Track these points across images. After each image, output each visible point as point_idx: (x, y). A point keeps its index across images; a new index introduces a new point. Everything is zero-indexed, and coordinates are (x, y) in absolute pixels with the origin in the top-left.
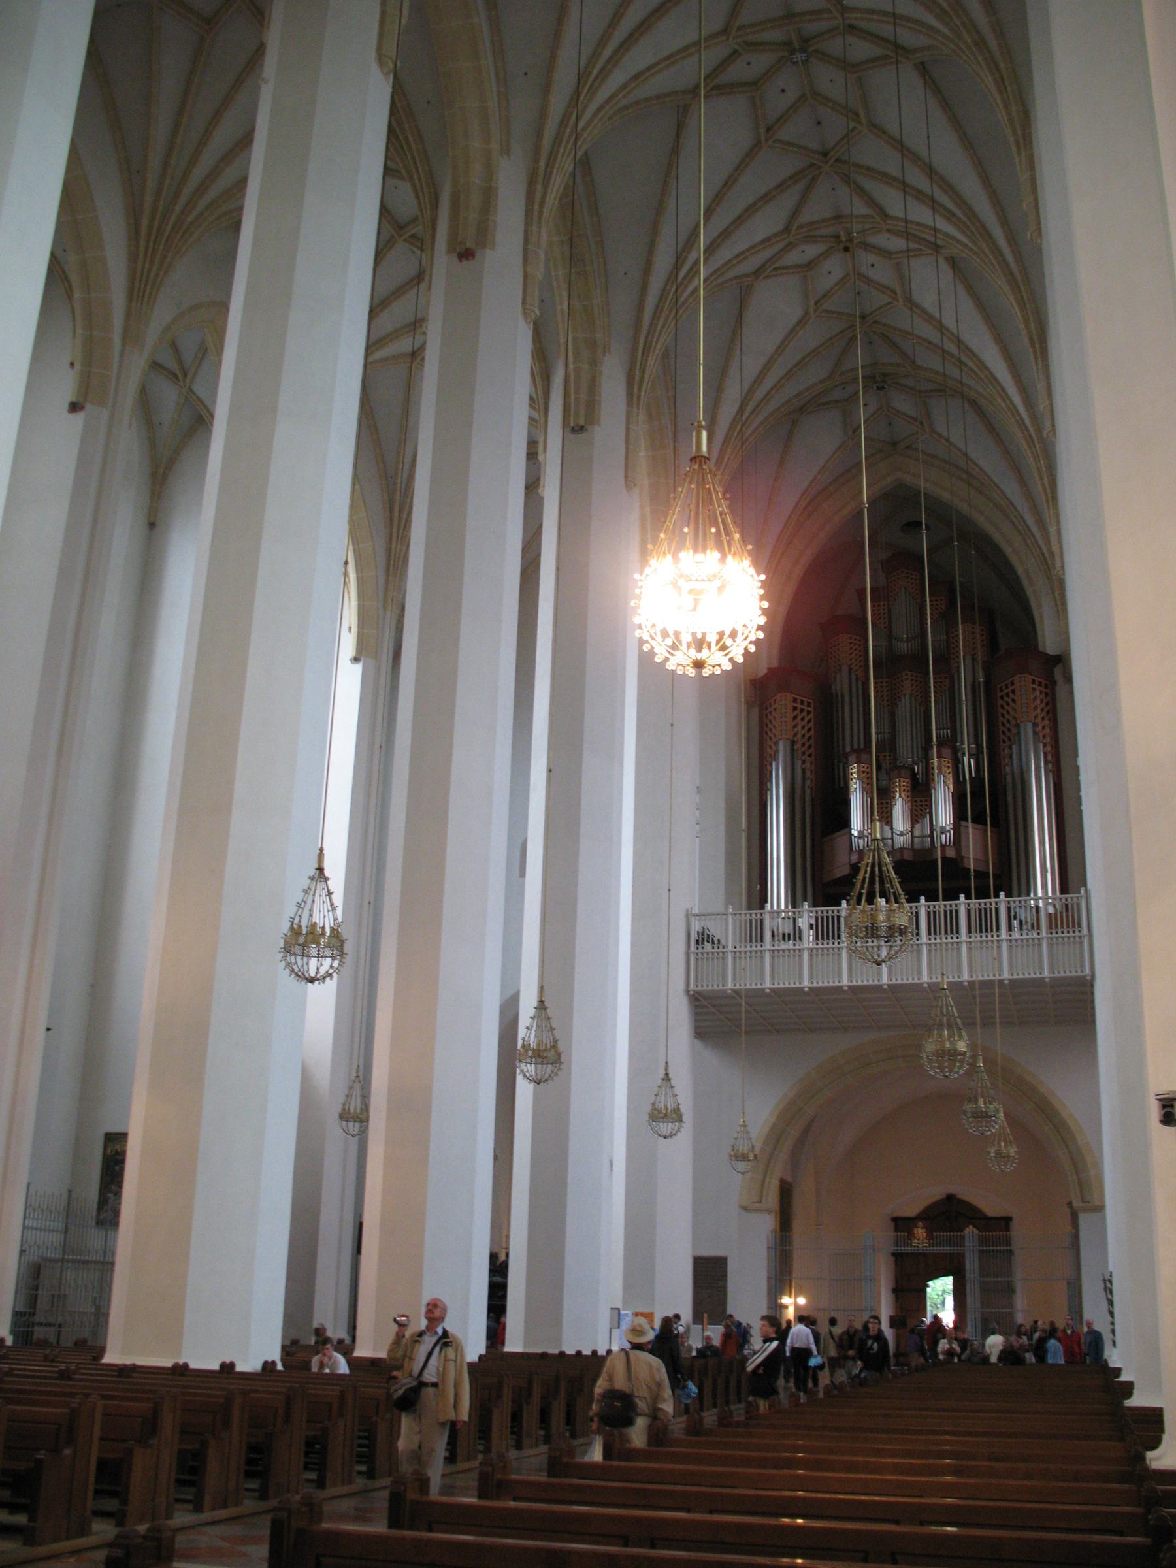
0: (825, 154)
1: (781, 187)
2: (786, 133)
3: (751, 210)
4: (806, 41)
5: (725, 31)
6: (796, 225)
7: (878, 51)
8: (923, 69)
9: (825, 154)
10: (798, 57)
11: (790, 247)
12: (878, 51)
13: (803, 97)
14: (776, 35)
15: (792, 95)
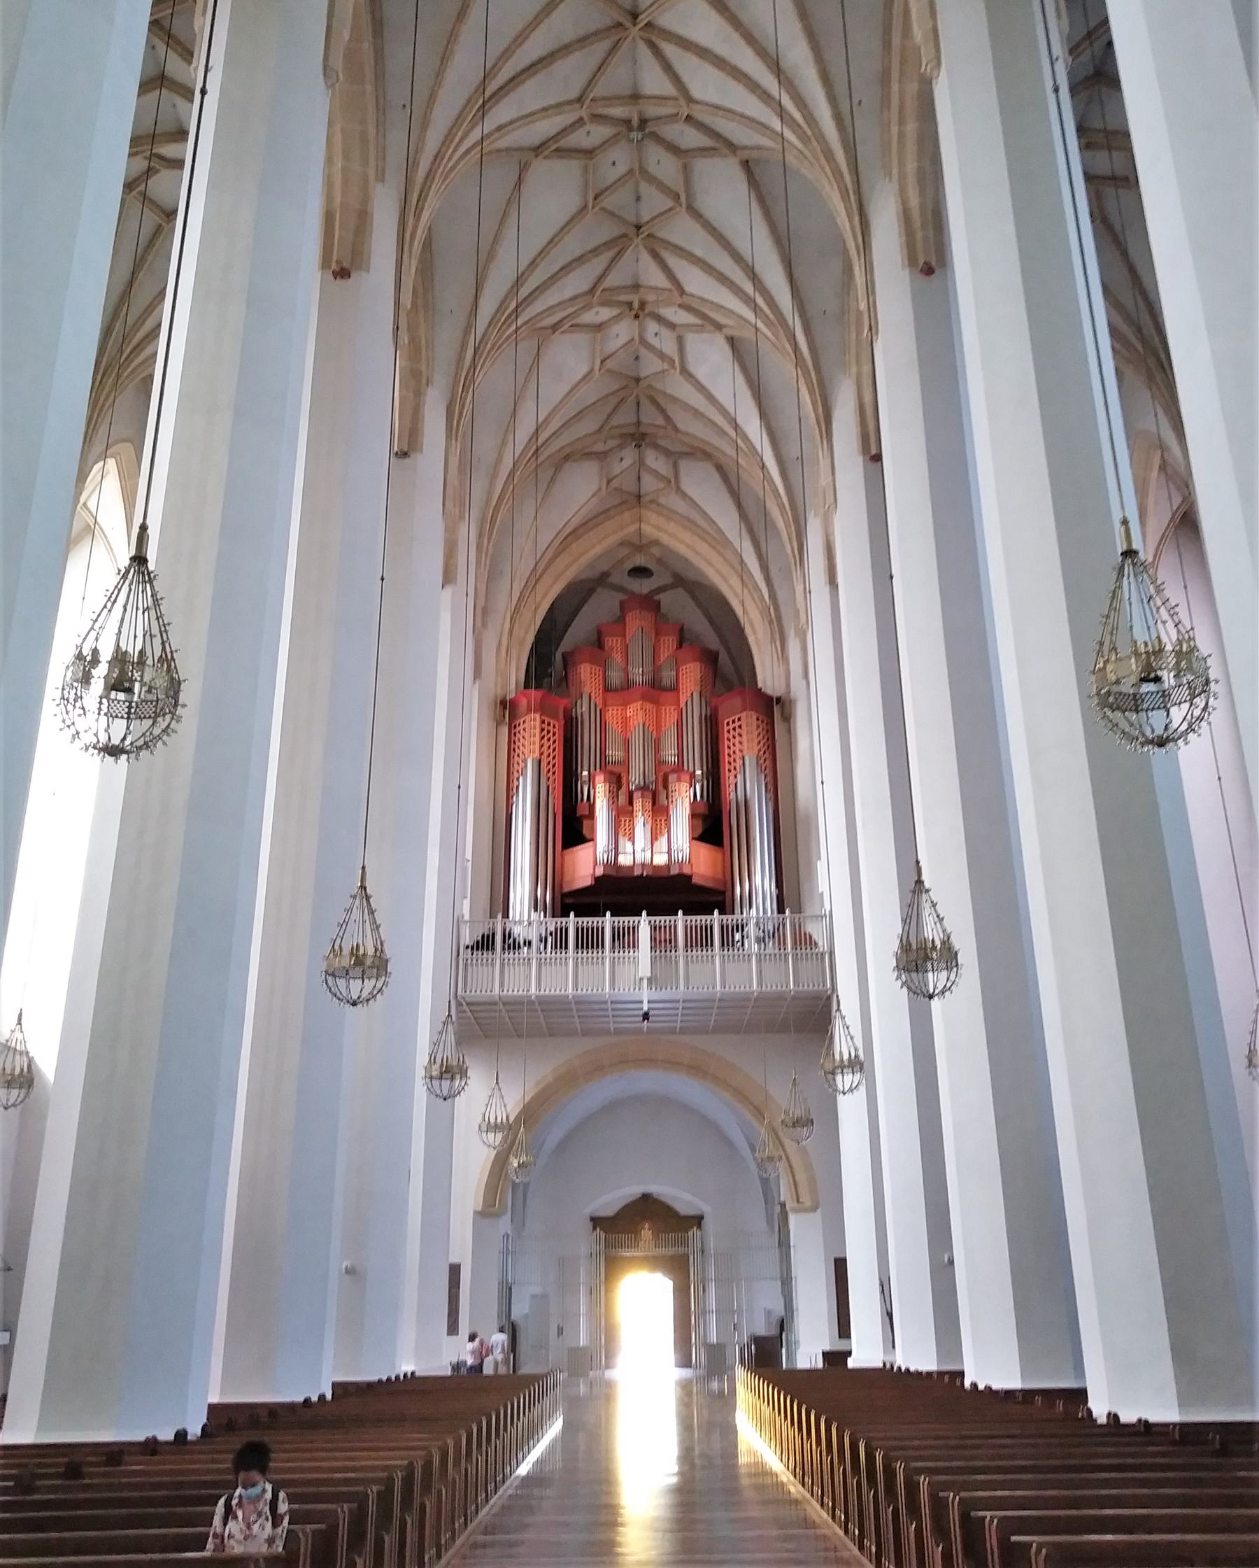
0: (638, 227)
1: (595, 251)
2: (608, 202)
3: (566, 269)
4: (643, 122)
5: (580, 100)
6: (601, 288)
7: (705, 141)
8: (746, 165)
9: (638, 227)
10: (635, 135)
11: (587, 307)
12: (705, 141)
13: (631, 171)
14: (618, 111)
15: (621, 169)
